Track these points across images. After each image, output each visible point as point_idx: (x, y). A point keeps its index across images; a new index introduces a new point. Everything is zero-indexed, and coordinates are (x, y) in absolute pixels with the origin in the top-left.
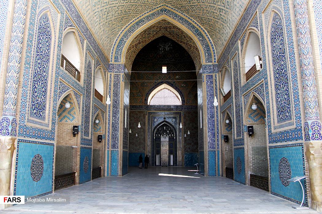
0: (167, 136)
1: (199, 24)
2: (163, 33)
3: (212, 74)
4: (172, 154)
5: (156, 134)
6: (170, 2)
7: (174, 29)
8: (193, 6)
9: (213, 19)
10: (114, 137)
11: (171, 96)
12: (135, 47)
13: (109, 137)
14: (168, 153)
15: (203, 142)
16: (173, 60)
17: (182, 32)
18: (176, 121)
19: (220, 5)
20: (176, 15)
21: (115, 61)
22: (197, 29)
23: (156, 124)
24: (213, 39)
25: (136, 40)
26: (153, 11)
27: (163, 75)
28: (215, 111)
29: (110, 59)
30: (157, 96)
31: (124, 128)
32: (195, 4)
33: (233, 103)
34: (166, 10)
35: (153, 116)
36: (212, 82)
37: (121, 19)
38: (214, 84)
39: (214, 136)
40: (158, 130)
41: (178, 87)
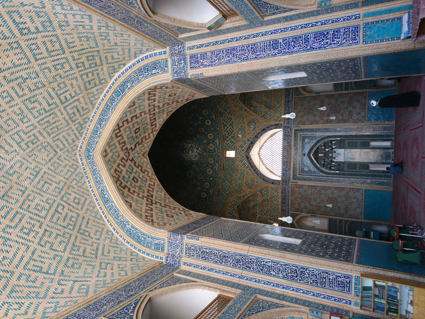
0: (335, 151)
1: (106, 90)
3: (188, 57)
5: (330, 169)
6: (71, 142)
7: (124, 136)
8: (59, 98)
12: (154, 206)
13: (318, 295)
14: (367, 150)
16: (217, 141)
18: (309, 137)
20: (95, 132)
22: (115, 92)
23: (312, 168)
27: (238, 156)
29: (157, 260)
35: (299, 172)
36: (204, 56)
37: (82, 234)
40: (324, 166)
41: (256, 134)
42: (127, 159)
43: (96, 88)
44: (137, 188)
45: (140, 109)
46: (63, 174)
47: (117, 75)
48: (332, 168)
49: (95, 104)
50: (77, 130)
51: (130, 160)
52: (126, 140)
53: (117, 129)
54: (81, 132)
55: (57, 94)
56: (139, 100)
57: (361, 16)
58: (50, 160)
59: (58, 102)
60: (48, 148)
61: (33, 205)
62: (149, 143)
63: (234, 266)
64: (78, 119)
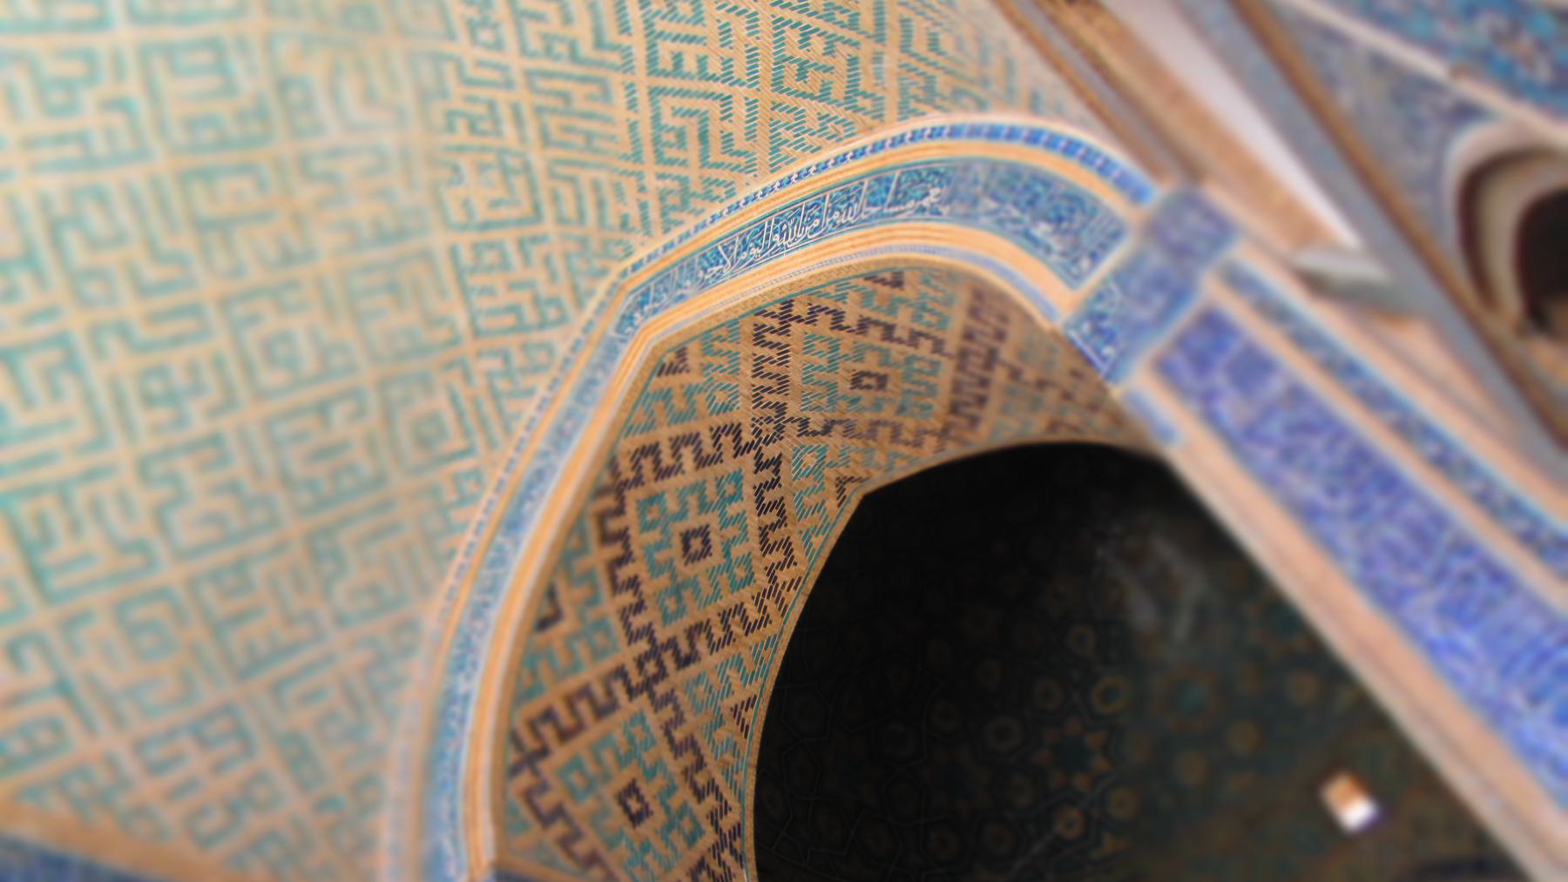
2: (830, 474)
6: (613, 220)
22: (881, 178)
36: (1253, 367)
42: (749, 446)
43: (823, 108)
44: (664, 580)
45: (916, 318)
46: (482, 303)
47: (934, 119)
49: (789, 161)
50: (662, 199)
51: (759, 456)
52: (795, 377)
53: (773, 315)
54: (673, 216)
55: (649, 25)
56: (926, 282)
58: (485, 226)
59: (640, 54)
60: (519, 183)
61: (271, 323)
62: (899, 464)
64: (684, 163)
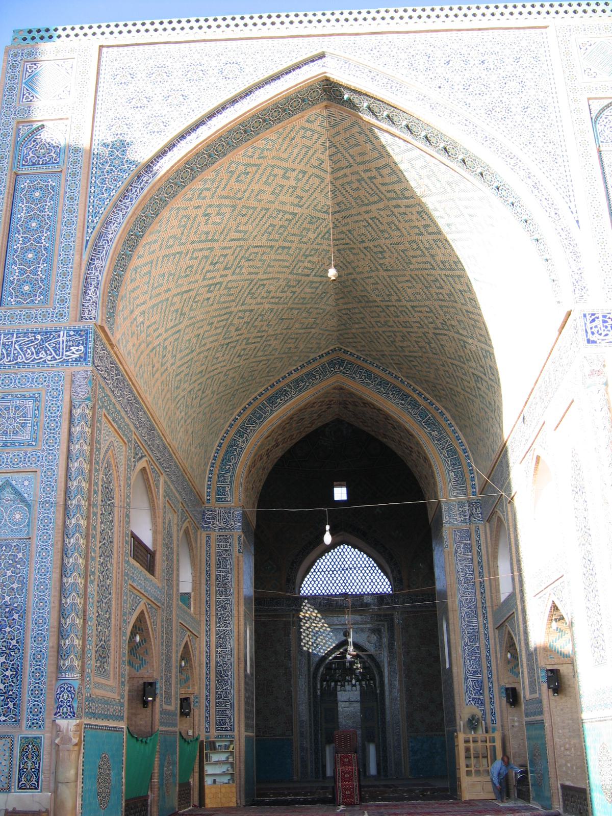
1: (428, 396)
4: (373, 741)
6: (354, 345)
7: (365, 409)
9: (462, 392)
10: (222, 701)
11: (363, 566)
12: (265, 458)
15: (453, 706)
17: (387, 417)
19: (474, 369)
20: (369, 375)
21: (218, 500)
24: (465, 435)
25: (269, 441)
26: (311, 367)
28: (481, 624)
30: (322, 567)
31: (246, 676)
32: (415, 354)
33: (517, 610)
34: (343, 361)
38: (475, 553)
39: (482, 688)
47: (448, 415)
48: (325, 683)
57: (494, 725)
63: (218, 603)
